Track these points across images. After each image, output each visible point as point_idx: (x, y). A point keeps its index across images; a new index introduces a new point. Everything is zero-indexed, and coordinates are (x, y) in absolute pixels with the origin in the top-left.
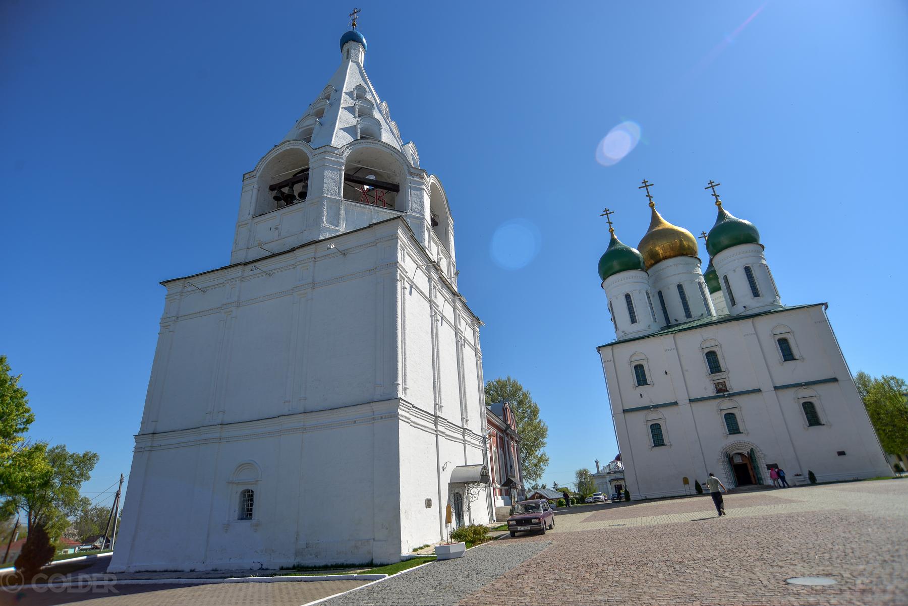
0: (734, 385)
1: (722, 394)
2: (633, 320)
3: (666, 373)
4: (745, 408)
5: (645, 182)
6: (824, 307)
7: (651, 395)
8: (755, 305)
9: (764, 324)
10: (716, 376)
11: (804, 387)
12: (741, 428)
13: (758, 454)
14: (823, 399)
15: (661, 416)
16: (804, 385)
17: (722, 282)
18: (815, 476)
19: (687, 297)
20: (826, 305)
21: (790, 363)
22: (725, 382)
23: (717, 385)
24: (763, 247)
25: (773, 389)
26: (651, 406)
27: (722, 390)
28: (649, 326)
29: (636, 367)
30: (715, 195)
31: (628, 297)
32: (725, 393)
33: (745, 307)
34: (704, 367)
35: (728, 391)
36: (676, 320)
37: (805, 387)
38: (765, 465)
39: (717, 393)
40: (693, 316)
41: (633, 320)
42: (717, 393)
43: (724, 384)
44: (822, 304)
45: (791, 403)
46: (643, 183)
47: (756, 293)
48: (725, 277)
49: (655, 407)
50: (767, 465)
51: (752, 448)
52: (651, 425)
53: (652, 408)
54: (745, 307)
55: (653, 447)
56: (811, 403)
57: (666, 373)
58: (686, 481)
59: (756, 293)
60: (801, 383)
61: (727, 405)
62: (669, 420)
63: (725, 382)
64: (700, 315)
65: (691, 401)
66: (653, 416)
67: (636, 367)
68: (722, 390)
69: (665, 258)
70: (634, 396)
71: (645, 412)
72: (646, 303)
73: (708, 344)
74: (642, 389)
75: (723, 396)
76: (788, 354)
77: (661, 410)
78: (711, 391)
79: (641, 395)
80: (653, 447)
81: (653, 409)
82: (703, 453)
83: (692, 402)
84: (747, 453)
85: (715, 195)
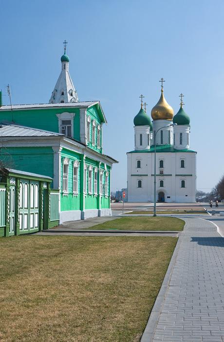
2: (141, 144)
4: (166, 180)
7: (141, 171)
8: (179, 147)
12: (164, 185)
14: (187, 180)
21: (183, 168)
23: (160, 171)
27: (162, 173)
41: (141, 144)
49: (141, 175)
61: (161, 178)
62: (144, 180)
66: (140, 178)
68: (162, 173)
69: (160, 119)
70: (136, 171)
76: (183, 166)
78: (158, 173)
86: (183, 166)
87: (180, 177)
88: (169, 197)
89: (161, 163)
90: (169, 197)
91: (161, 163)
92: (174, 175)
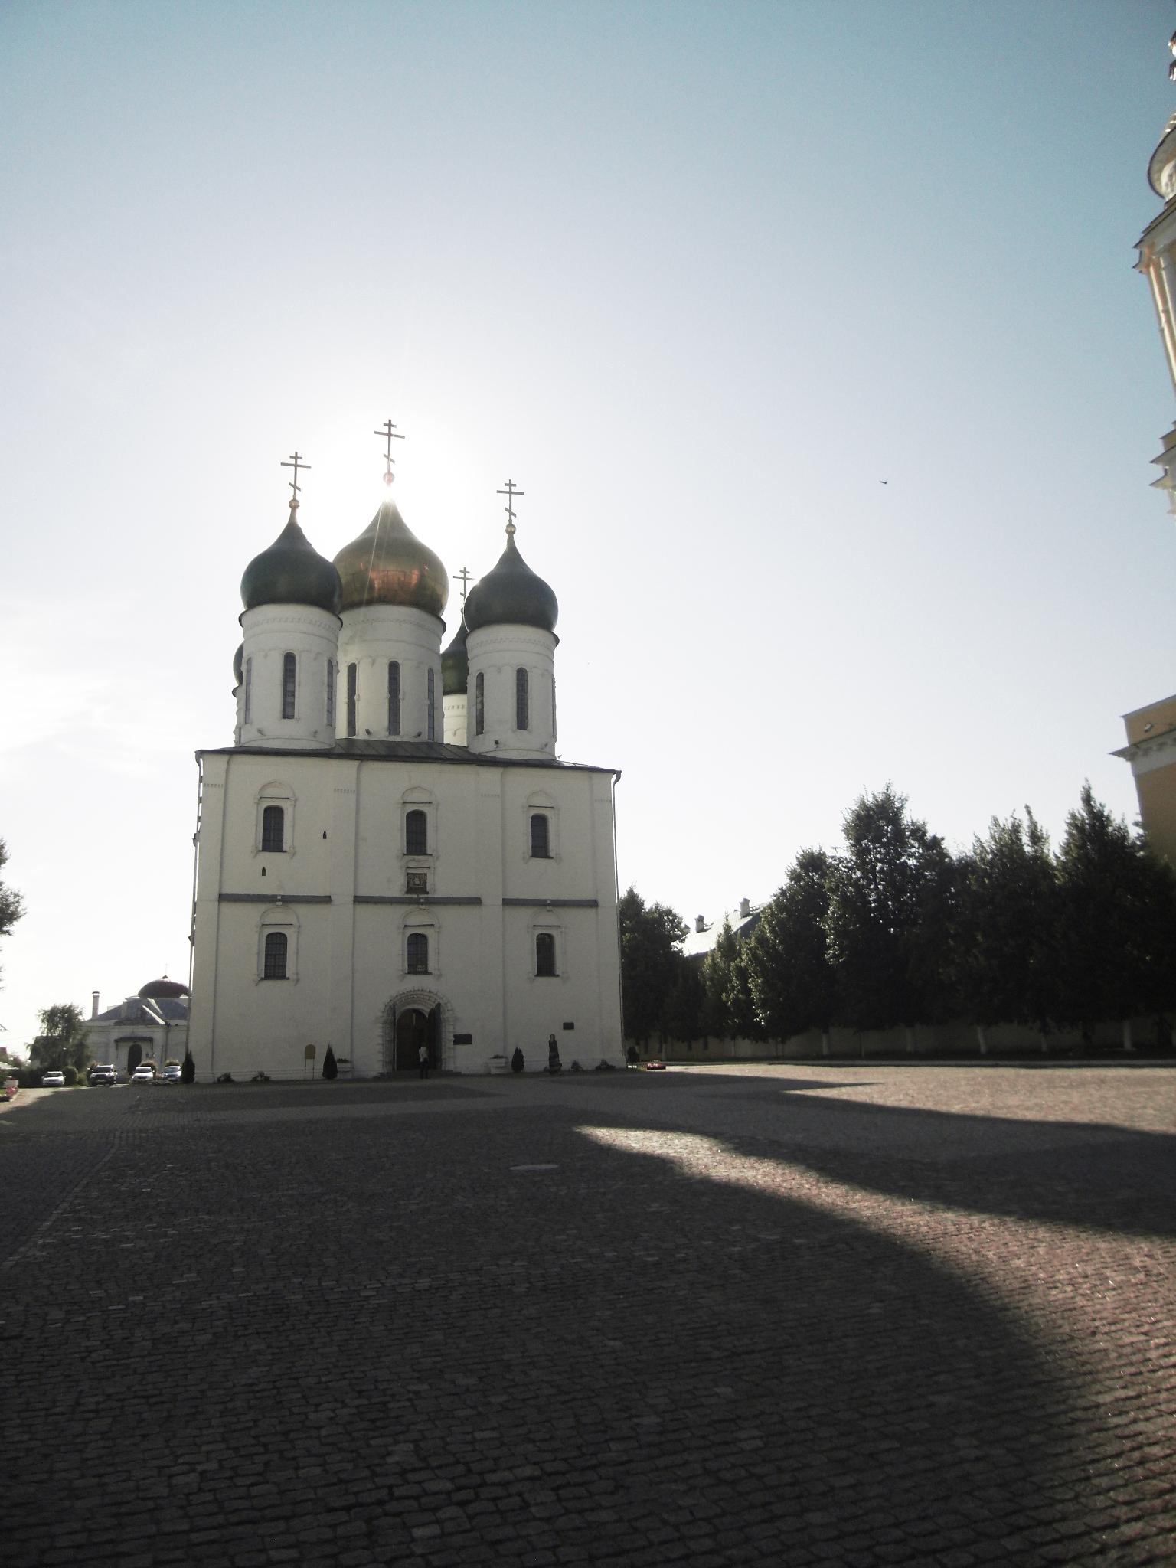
0: (441, 885)
1: (415, 896)
3: (325, 836)
5: (510, 484)
6: (615, 776)
8: (516, 745)
9: (523, 782)
10: (414, 860)
11: (548, 908)
13: (446, 1015)
15: (294, 921)
16: (549, 905)
17: (472, 681)
18: (524, 1060)
19: (401, 692)
20: (618, 773)
22: (426, 874)
23: (410, 877)
24: (557, 641)
25: (500, 902)
26: (279, 898)
27: (417, 890)
28: (316, 732)
29: (269, 811)
30: (509, 511)
31: (289, 659)
32: (421, 896)
33: (497, 742)
34: (398, 839)
35: (428, 893)
36: (368, 732)
37: (551, 908)
38: (452, 1035)
39: (407, 893)
40: (401, 732)
41: (287, 711)
42: (407, 893)
43: (423, 878)
44: (613, 772)
45: (523, 930)
46: (506, 485)
47: (522, 723)
48: (481, 677)
49: (287, 900)
50: (455, 1036)
51: (439, 1004)
52: (270, 936)
53: (279, 900)
54: (497, 742)
55: (262, 979)
56: (550, 936)
57: (325, 836)
58: (310, 1052)
59: (522, 723)
60: (546, 900)
61: (418, 917)
63: (426, 874)
64: (416, 733)
65: (358, 900)
67: (268, 810)
68: (417, 890)
71: (262, 907)
72: (323, 684)
73: (416, 797)
74: (269, 859)
75: (417, 902)
76: (540, 847)
77: (302, 910)
78: (396, 888)
79: (264, 870)
80: (262, 979)
81: (280, 903)
82: (353, 1002)
83: (359, 902)
84: (428, 1010)
85: (509, 511)
86: (540, 847)
87: (523, 917)
88: (464, 1040)
89: (416, 825)
90: (464, 1040)
91: (416, 825)
92: (492, 901)
